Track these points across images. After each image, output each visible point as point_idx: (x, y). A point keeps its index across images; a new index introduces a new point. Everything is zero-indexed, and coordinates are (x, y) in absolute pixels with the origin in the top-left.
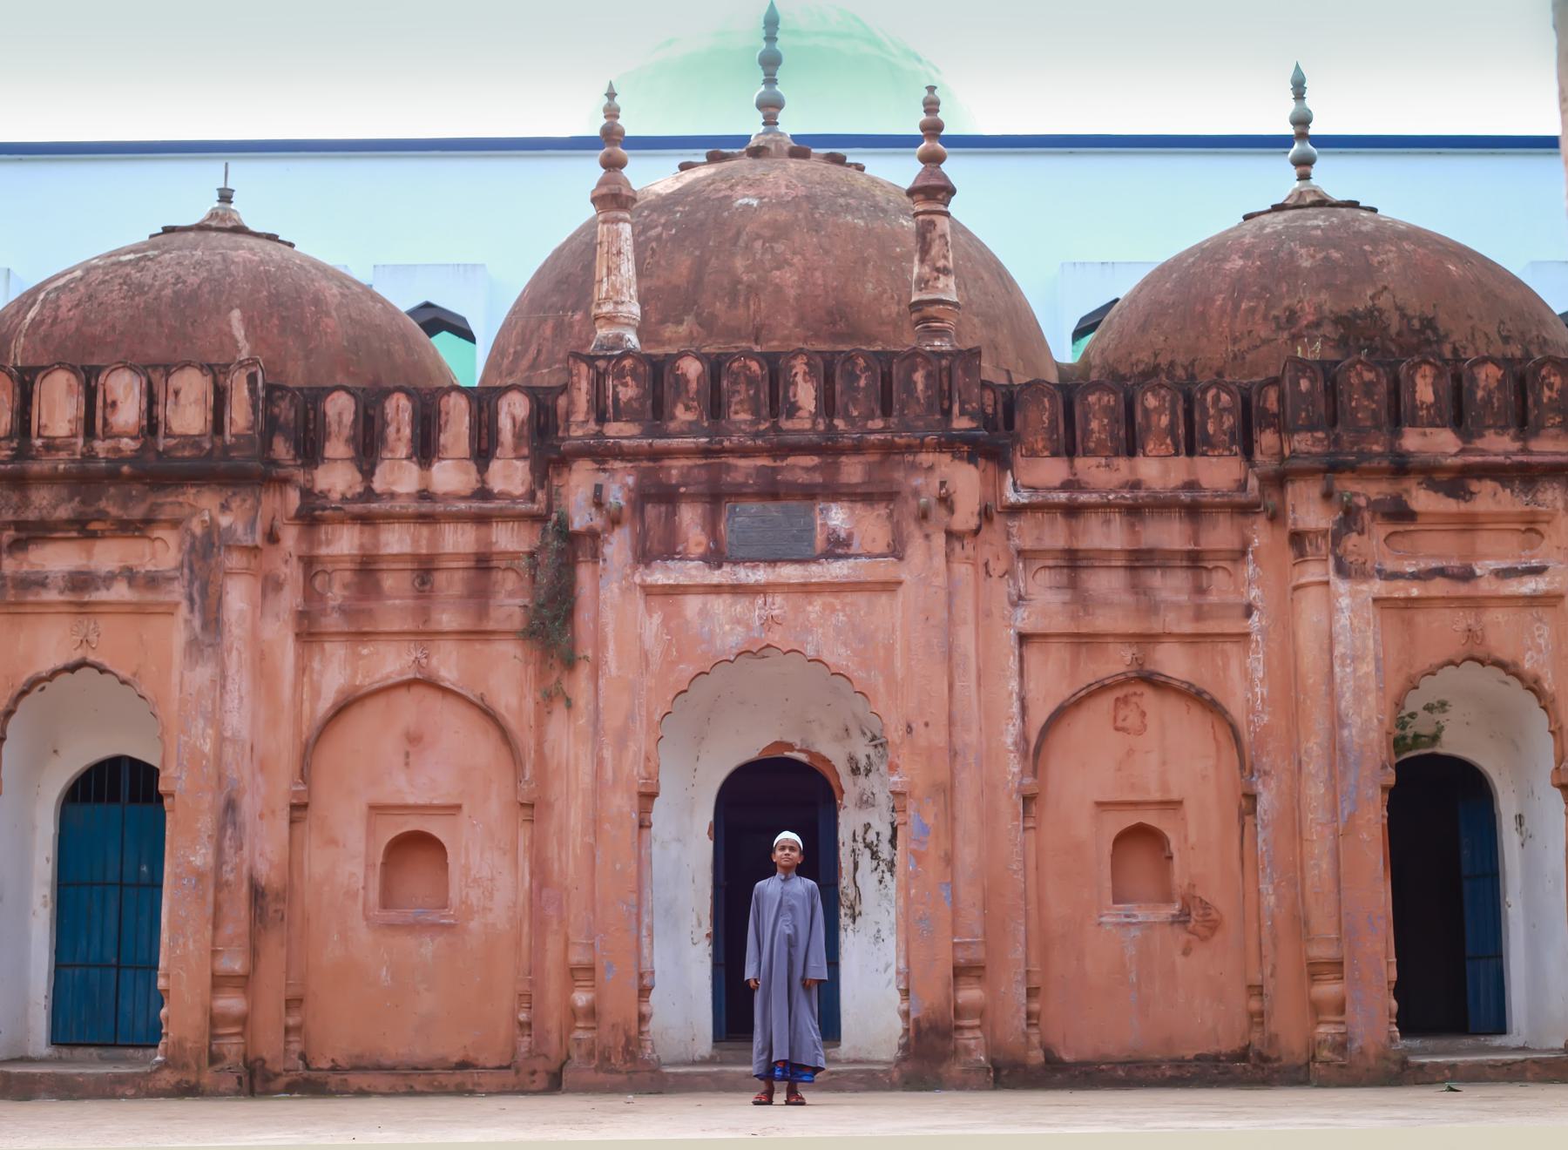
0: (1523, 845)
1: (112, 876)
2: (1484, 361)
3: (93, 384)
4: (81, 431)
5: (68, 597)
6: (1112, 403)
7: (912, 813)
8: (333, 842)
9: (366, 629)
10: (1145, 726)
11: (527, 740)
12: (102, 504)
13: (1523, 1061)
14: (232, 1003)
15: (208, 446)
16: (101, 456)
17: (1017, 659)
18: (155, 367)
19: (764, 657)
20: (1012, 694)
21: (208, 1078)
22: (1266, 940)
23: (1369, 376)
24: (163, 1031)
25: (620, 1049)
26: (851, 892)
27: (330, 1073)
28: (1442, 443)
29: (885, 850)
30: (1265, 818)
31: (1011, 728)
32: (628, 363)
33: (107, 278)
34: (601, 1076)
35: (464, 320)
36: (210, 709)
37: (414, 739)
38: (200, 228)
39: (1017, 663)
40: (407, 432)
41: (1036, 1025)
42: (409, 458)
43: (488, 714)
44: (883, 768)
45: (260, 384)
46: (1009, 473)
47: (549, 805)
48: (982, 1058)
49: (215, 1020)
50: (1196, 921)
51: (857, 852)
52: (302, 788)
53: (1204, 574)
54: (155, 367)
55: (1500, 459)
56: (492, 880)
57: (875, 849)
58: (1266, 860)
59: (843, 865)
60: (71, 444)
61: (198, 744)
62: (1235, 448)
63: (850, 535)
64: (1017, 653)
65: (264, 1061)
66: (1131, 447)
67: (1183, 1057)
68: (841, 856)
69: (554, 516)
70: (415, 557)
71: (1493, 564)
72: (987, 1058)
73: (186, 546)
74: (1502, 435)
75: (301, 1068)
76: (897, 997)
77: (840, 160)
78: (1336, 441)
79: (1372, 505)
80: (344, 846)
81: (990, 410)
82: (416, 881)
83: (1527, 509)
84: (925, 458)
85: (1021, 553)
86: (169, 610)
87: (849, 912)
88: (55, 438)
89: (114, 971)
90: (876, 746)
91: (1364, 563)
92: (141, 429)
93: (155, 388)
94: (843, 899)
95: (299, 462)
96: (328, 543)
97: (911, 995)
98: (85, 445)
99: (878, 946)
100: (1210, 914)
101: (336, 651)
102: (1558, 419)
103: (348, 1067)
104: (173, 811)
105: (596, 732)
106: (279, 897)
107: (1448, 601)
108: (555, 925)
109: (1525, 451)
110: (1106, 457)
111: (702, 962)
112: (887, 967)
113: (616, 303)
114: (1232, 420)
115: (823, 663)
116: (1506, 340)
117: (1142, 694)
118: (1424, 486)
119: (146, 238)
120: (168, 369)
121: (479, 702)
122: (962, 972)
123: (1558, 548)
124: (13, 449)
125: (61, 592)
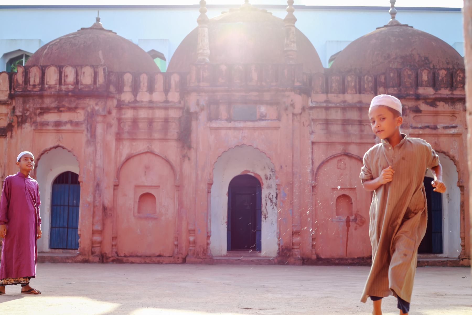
0: (448, 202)
1: (66, 204)
2: (442, 69)
3: (61, 70)
4: (58, 83)
5: (54, 128)
6: (339, 79)
8: (125, 195)
9: (135, 138)
11: (178, 169)
12: (64, 103)
13: (447, 261)
14: (97, 238)
15: (92, 87)
16: (64, 90)
17: (311, 149)
18: (78, 66)
20: (309, 158)
21: (91, 258)
23: (410, 73)
24: (79, 245)
25: (202, 252)
26: (265, 211)
27: (124, 257)
28: (430, 91)
29: (274, 200)
31: (309, 167)
32: (206, 66)
34: (197, 259)
35: (163, 54)
37: (147, 168)
38: (91, 28)
40: (146, 84)
41: (314, 248)
42: (147, 91)
43: (167, 161)
44: (274, 178)
46: (310, 98)
48: (300, 257)
51: (267, 200)
53: (363, 126)
54: (78, 66)
55: (445, 96)
57: (272, 200)
60: (55, 87)
62: (372, 92)
63: (266, 114)
64: (311, 147)
65: (106, 254)
66: (344, 91)
69: (186, 108)
70: (148, 119)
71: (443, 125)
72: (301, 257)
74: (446, 89)
76: (276, 240)
77: (265, 12)
78: (400, 91)
79: (410, 108)
81: (305, 80)
83: (452, 110)
84: (287, 93)
85: (313, 120)
86: (82, 132)
87: (264, 216)
88: (51, 85)
89: (66, 229)
90: (272, 172)
91: (407, 124)
92: (74, 83)
93: (78, 72)
94: (263, 213)
95: (117, 92)
98: (59, 87)
100: (362, 219)
102: (462, 85)
103: (128, 255)
107: (430, 135)
109: (452, 94)
110: (337, 94)
114: (371, 84)
116: (448, 63)
118: (424, 103)
119: (76, 31)
120: (82, 66)
121: (165, 158)
122: (295, 233)
123: (461, 121)
124: (40, 88)
125: (53, 127)
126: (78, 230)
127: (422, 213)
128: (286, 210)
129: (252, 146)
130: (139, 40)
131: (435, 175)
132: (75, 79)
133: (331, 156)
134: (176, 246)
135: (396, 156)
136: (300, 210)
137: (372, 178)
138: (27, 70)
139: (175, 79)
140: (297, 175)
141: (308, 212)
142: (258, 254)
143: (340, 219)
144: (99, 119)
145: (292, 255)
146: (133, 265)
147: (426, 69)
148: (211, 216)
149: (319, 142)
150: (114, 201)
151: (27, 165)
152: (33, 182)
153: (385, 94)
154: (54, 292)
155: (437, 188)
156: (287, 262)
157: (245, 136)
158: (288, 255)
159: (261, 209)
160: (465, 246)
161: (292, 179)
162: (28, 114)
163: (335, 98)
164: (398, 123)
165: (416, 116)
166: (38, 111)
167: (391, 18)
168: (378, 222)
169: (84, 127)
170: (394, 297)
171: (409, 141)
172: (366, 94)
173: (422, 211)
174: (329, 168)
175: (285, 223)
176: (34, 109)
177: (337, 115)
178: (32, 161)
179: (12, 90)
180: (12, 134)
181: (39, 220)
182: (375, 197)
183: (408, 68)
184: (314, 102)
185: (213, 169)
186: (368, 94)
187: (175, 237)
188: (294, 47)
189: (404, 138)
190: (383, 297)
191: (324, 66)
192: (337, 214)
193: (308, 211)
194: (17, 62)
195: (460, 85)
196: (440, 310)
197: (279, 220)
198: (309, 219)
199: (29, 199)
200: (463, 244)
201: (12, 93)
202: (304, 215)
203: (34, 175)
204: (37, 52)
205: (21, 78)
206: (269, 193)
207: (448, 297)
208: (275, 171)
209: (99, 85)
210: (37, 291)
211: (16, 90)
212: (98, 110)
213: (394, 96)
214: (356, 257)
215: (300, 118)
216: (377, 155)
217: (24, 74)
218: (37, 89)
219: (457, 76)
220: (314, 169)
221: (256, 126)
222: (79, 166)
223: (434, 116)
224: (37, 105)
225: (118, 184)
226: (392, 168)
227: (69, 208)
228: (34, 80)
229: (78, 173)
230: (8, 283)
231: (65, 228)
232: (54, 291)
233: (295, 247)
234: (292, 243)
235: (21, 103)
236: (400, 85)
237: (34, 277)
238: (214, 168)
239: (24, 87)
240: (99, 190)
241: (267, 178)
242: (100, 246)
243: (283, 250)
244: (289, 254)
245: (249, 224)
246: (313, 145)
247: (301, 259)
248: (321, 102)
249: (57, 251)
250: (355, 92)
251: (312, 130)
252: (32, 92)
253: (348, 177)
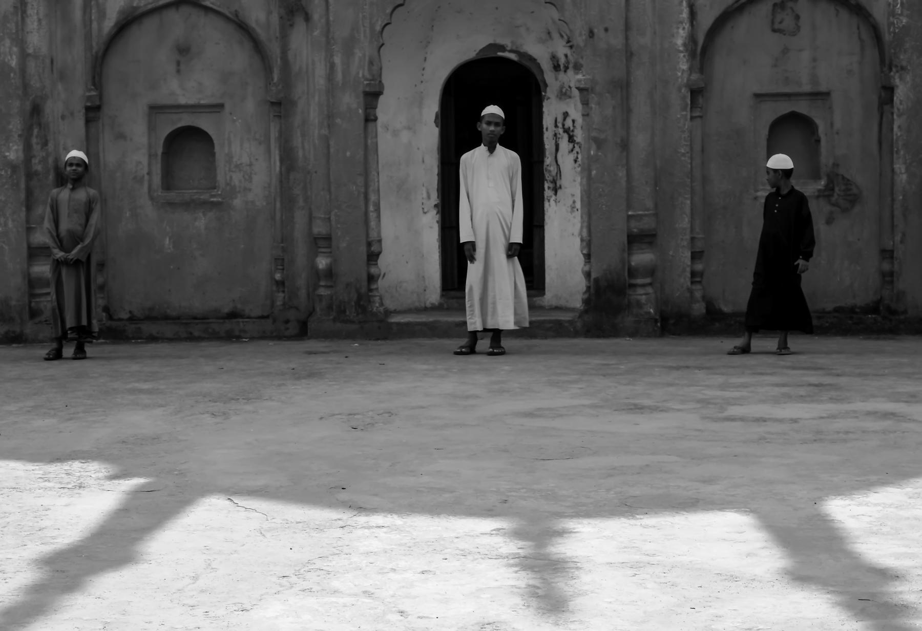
7: (593, 106)
8: (121, 136)
10: (798, 28)
11: (274, 49)
21: (29, 329)
22: (898, 213)
25: (353, 303)
30: (901, 107)
31: (681, 31)
36: (14, 31)
37: (184, 51)
41: (700, 282)
43: (242, 27)
47: (293, 103)
48: (652, 311)
49: (32, 283)
50: (838, 195)
52: (93, 93)
56: (251, 165)
58: (900, 143)
59: (546, 147)
61: (6, 60)
68: (545, 139)
75: (104, 319)
80: (131, 140)
97: (592, 260)
99: (574, 214)
100: (850, 190)
105: (328, 43)
108: (301, 202)
111: (431, 227)
121: (235, 19)
122: (635, 240)
134: (281, 284)
206: (564, 114)
214: (830, 307)
225: (98, 103)
233: (639, 281)
234: (629, 270)
238: (383, 44)
240: (40, 125)
241: (556, 68)
247: (657, 317)
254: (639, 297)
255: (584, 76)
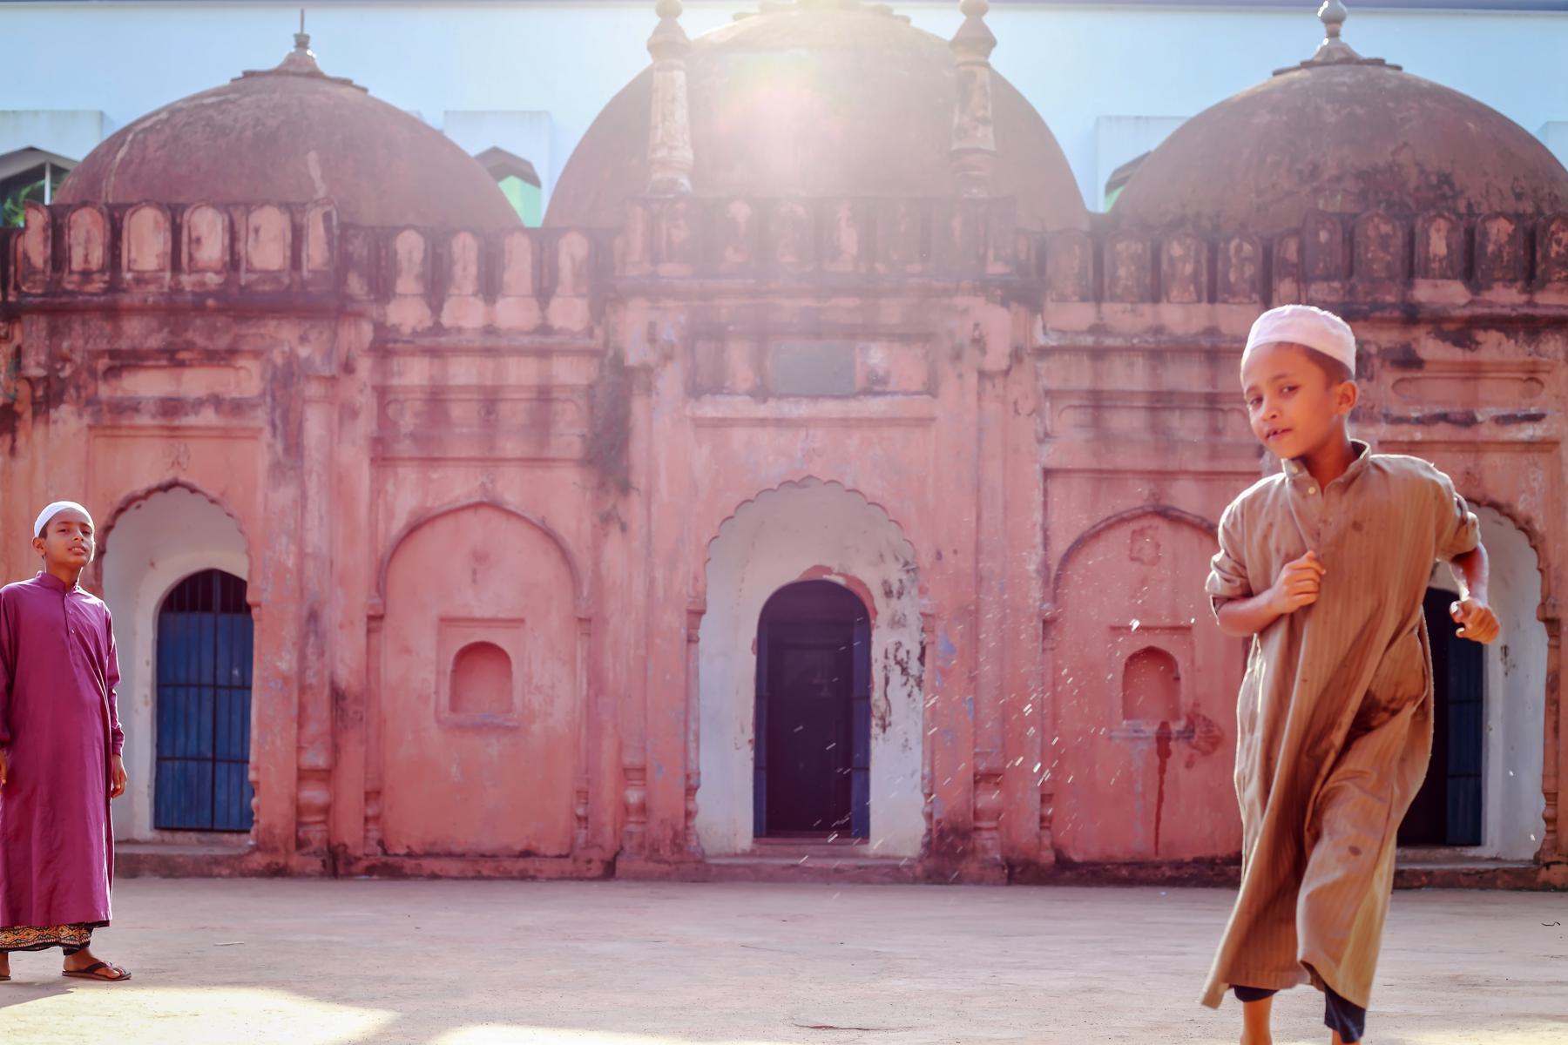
0: (1506, 674)
2: (1497, 215)
3: (178, 220)
5: (160, 421)
6: (1140, 251)
8: (407, 650)
9: (436, 455)
11: (584, 561)
12: (190, 335)
13: (1495, 870)
14: (315, 794)
15: (286, 280)
16: (188, 288)
17: (1042, 492)
18: (236, 205)
19: (804, 487)
20: (1035, 525)
23: (1386, 229)
24: (255, 818)
26: (882, 704)
27: (406, 859)
28: (1452, 295)
29: (914, 666)
32: (681, 206)
33: (191, 119)
35: (529, 165)
39: (1041, 496)
40: (473, 270)
41: (1048, 828)
42: (475, 295)
43: (549, 535)
44: (914, 592)
45: (335, 222)
46: (1039, 317)
48: (998, 857)
51: (888, 668)
53: (1220, 416)
54: (236, 205)
55: (1506, 311)
56: (553, 687)
57: (905, 666)
62: (1255, 297)
63: (888, 373)
64: (1041, 486)
65: (345, 846)
66: (1156, 293)
67: (1182, 860)
70: (481, 389)
71: (1494, 411)
72: (1002, 857)
73: (268, 375)
74: (1509, 288)
76: (922, 798)
77: (887, 12)
79: (1384, 353)
81: (1023, 256)
82: (482, 689)
83: (1530, 359)
84: (961, 301)
85: (1049, 394)
86: (254, 435)
87: (880, 722)
88: (143, 272)
90: (908, 571)
91: (1372, 408)
92: (225, 265)
94: (875, 711)
95: (372, 297)
96: (400, 374)
98: (172, 278)
101: (409, 475)
102: (1564, 274)
103: (422, 853)
104: (260, 620)
106: (358, 700)
107: (1449, 444)
109: (1530, 303)
110: (1132, 303)
112: (913, 774)
113: (672, 148)
114: (1252, 268)
115: (860, 493)
116: (1519, 197)
117: (1157, 528)
118: (1433, 335)
120: (249, 207)
121: (540, 524)
123: (1557, 397)
124: (105, 282)
125: (154, 417)
126: (251, 766)
127: (1414, 709)
128: (954, 699)
129: (839, 483)
130: (446, 113)
131: (1465, 581)
132: (228, 252)
133: (1109, 518)
134: (583, 820)
135: (1331, 519)
136: (1001, 702)
137: (1248, 594)
138: (59, 221)
139: (572, 250)
140: (993, 583)
141: (1026, 708)
142: (858, 847)
143: (1136, 731)
144: (313, 389)
145: (974, 851)
146: (438, 882)
147: (1442, 216)
148: (698, 720)
149: (1068, 471)
150: (370, 668)
151: (70, 550)
152: (94, 607)
153: (1298, 302)
154: (175, 973)
155: (1469, 626)
156: (956, 874)
157: (814, 450)
158: (958, 851)
159: (868, 697)
160: (1559, 822)
161: (975, 596)
162: (67, 372)
163: (1127, 319)
164: (1340, 404)
165: (1402, 380)
166: (103, 364)
167: (1325, 35)
168: (1264, 740)
169: (260, 418)
170: (1312, 988)
171: (1377, 467)
172: (1234, 303)
173: (1415, 704)
174: (1101, 558)
175: (949, 744)
176: (86, 355)
177: (1130, 377)
178: (86, 533)
179: (11, 291)
180: (14, 440)
181: (117, 734)
182: (1258, 657)
183: (1381, 212)
184: (1054, 330)
185: (706, 562)
186: (1240, 303)
187: (578, 792)
188: (985, 138)
189: (1362, 456)
190: (1276, 991)
191: (1090, 207)
192: (1128, 715)
193: (1030, 706)
194: (25, 191)
195: (1560, 273)
196: (1466, 1032)
197: (930, 734)
198: (1032, 730)
199: (80, 663)
200: (1550, 813)
201: (11, 299)
202: (1014, 718)
203: (94, 582)
204: (93, 157)
205: (41, 248)
207: (1496, 988)
208: (918, 568)
209: (309, 271)
210: (117, 970)
211: (24, 289)
212: (308, 359)
213: (1330, 311)
214: (1188, 857)
215: (1005, 387)
216: (1267, 514)
217: (50, 233)
218: (97, 285)
219: (1550, 240)
220: (1050, 562)
221: (853, 415)
222: (248, 553)
223: (1467, 378)
224: (98, 341)
225: (381, 612)
226: (1317, 560)
227: (215, 694)
228: (86, 256)
229: (243, 575)
230: (17, 944)
231: (206, 760)
232: (172, 971)
233: (984, 824)
235: (44, 333)
236: (1350, 272)
237: (106, 923)
238: (709, 560)
239: (51, 278)
240: (316, 633)
242: (324, 822)
243: (942, 834)
244: (961, 848)
245: (828, 748)
246: (1049, 480)
248: (1077, 333)
249: (179, 837)
250: (1194, 297)
251: (1046, 429)
252: (80, 298)
253: (1164, 589)
254: (985, 842)
255: (930, 600)
